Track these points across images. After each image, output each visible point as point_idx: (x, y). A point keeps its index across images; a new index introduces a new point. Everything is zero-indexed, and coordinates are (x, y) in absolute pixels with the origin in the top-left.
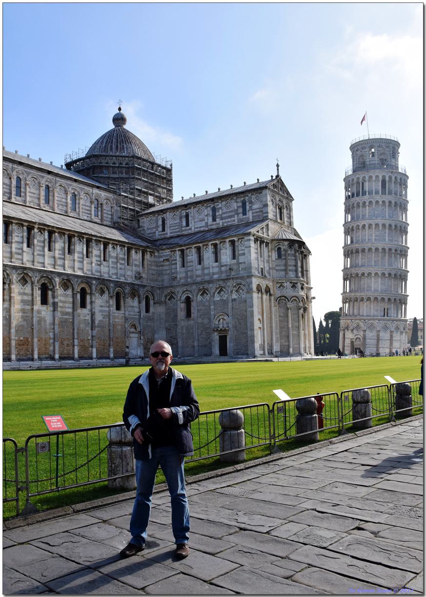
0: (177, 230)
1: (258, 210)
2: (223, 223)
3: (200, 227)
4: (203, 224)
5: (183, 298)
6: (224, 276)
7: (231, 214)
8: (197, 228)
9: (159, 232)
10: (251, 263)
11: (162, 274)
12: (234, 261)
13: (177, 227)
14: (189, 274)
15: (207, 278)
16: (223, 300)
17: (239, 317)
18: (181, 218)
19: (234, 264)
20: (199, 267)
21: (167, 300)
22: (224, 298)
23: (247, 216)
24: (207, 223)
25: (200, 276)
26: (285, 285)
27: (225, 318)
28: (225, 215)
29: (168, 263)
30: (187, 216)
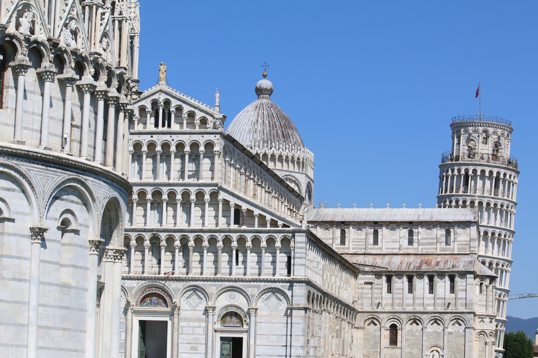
0: (362, 247)
1: (464, 243)
2: (422, 249)
3: (393, 249)
4: (397, 245)
5: (388, 325)
6: (440, 309)
7: (431, 241)
8: (388, 249)
9: (336, 245)
10: (472, 300)
11: (362, 298)
12: (453, 295)
13: (361, 243)
14: (397, 301)
15: (420, 309)
16: (437, 332)
17: (455, 350)
18: (367, 234)
19: (452, 299)
20: (411, 295)
21: (366, 325)
22: (439, 331)
23: (452, 246)
24: (400, 246)
25: (410, 306)
26: (485, 320)
27: (439, 350)
28: (425, 241)
29: (370, 286)
30: (376, 233)
